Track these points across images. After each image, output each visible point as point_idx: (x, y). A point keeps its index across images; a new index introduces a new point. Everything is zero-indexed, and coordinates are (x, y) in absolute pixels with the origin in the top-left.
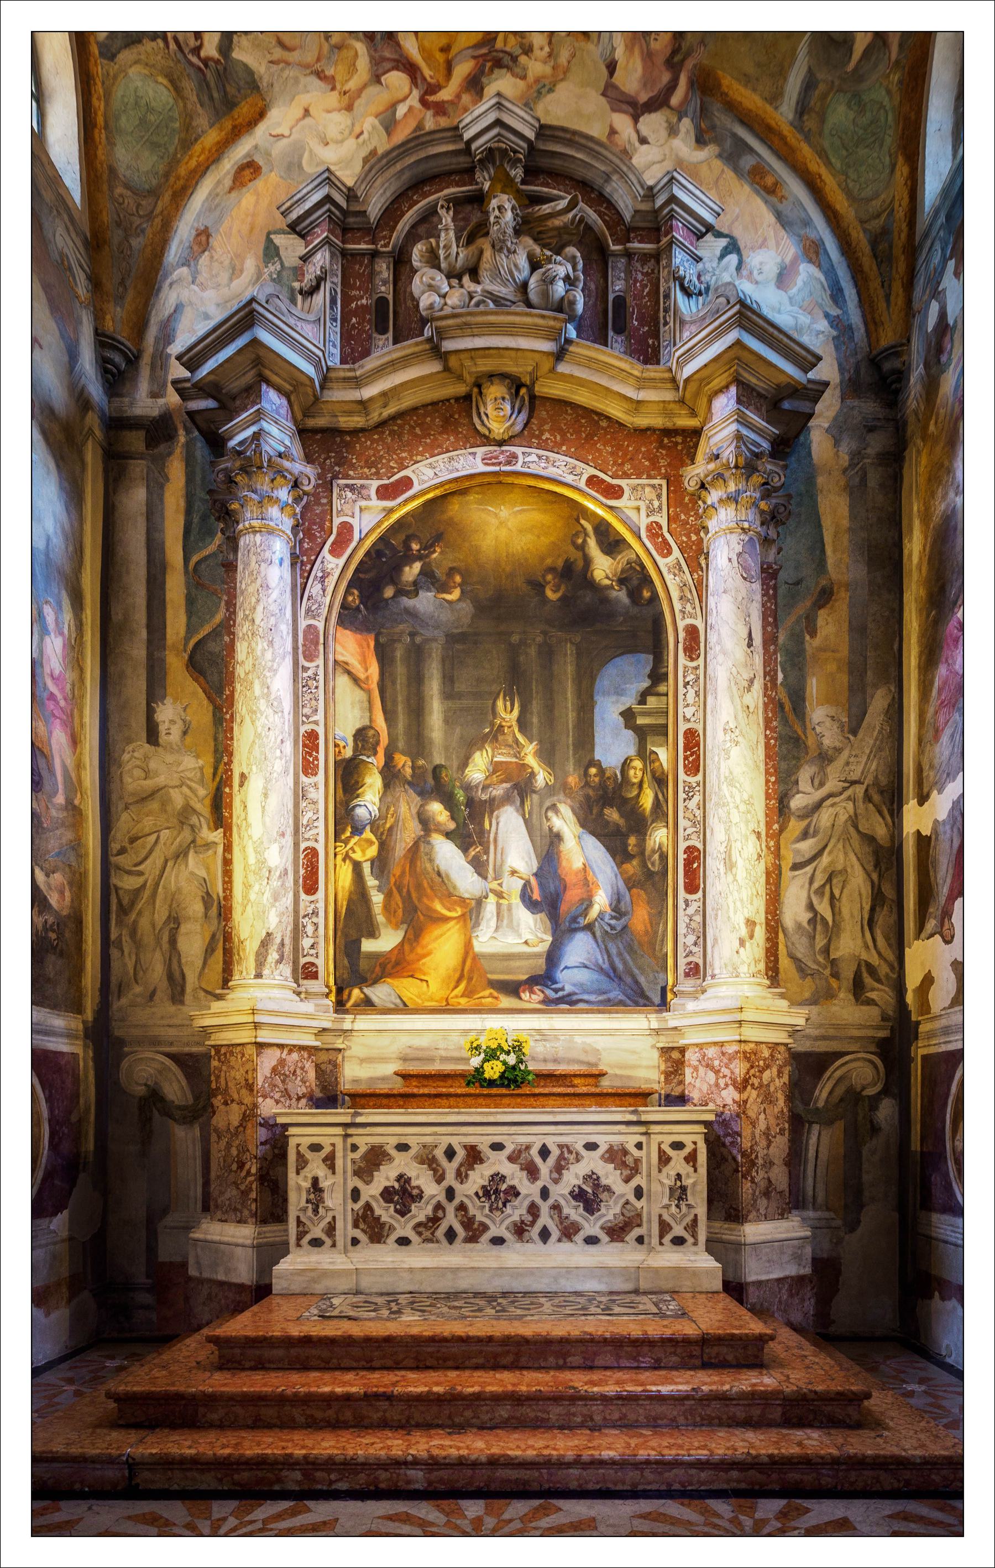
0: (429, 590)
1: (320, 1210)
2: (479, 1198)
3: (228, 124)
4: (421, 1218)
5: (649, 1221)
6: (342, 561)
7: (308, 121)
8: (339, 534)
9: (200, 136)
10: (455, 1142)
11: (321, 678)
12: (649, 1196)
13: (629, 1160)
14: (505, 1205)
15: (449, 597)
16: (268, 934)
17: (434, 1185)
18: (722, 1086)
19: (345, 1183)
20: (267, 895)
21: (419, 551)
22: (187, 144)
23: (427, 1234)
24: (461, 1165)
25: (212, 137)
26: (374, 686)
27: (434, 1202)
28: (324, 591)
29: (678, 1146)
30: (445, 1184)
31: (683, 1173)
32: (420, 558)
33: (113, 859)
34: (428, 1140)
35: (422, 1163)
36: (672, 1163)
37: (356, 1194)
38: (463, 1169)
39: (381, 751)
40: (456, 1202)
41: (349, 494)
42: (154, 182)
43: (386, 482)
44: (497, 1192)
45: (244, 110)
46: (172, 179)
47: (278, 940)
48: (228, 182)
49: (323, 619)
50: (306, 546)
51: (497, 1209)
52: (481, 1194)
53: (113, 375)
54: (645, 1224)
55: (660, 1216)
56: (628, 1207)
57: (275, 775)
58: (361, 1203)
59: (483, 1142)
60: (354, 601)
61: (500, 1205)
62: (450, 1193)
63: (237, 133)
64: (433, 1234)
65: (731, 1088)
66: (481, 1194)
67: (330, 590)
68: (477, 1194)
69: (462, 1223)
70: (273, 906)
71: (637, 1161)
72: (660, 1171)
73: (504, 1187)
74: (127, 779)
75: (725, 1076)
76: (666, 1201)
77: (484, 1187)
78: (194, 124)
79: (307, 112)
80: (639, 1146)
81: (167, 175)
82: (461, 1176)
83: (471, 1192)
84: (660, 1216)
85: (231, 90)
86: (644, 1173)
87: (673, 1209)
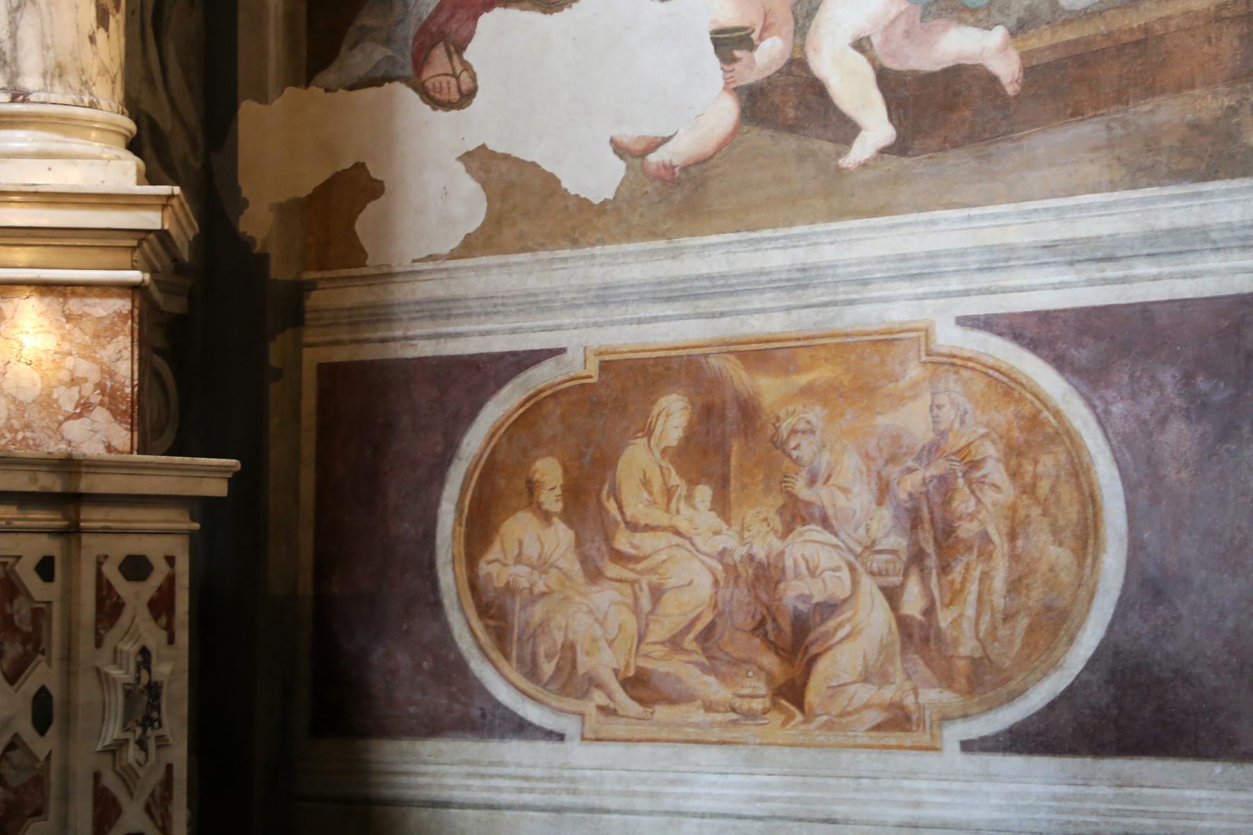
5: (66, 796)
12: (67, 719)
13: (20, 611)
18: (69, 407)
29: (136, 568)
31: (152, 645)
36: (124, 619)
54: (53, 808)
55: (97, 776)
56: (16, 756)
65: (101, 416)
71: (40, 614)
72: (99, 643)
75: (74, 382)
76: (113, 731)
80: (45, 568)
84: (97, 776)
86: (56, 650)
87: (132, 754)
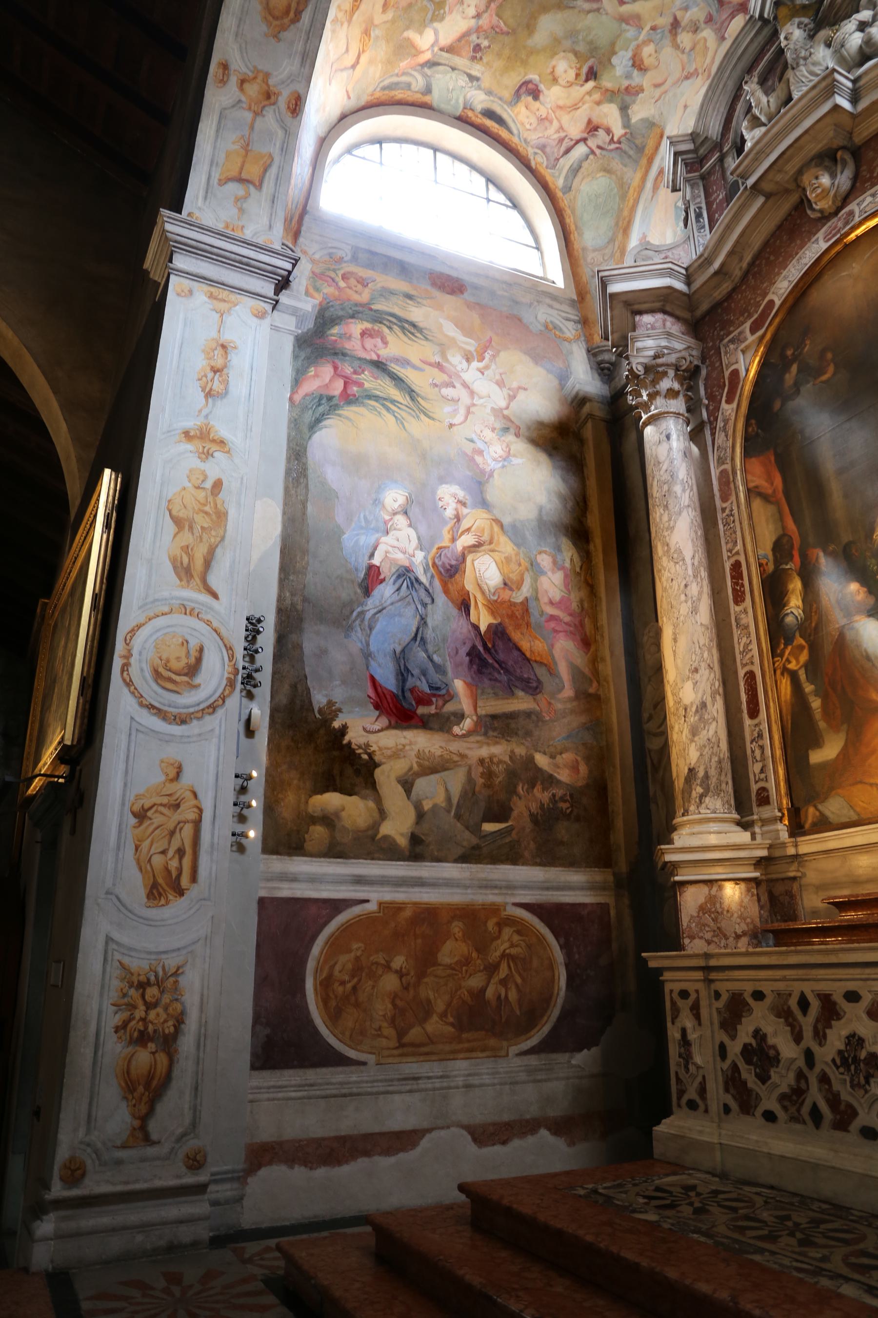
0: (808, 382)
1: (691, 1067)
2: (838, 1068)
3: (644, 161)
4: (784, 1088)
6: (735, 405)
7: (688, 110)
8: (730, 383)
9: (630, 184)
10: (808, 989)
11: (735, 511)
14: (868, 1082)
15: (825, 377)
16: (691, 770)
17: (793, 1044)
19: (713, 1037)
20: (686, 732)
21: (793, 354)
22: (623, 197)
23: (793, 1110)
24: (818, 1020)
25: (639, 175)
26: (781, 495)
27: (794, 1067)
28: (726, 436)
30: (804, 1044)
32: (795, 358)
33: (646, 727)
34: (781, 986)
35: (778, 1016)
37: (723, 1051)
38: (820, 1026)
39: (796, 553)
40: (817, 1069)
41: (732, 346)
42: (610, 234)
43: (756, 316)
44: (856, 1060)
45: (651, 144)
46: (621, 223)
47: (701, 774)
48: (651, 194)
49: (729, 461)
50: (711, 408)
51: (859, 1085)
52: (838, 1062)
53: (609, 369)
57: (682, 618)
58: (728, 1062)
59: (837, 991)
60: (753, 430)
61: (862, 1081)
62: (809, 1056)
63: (650, 161)
64: (798, 1111)
66: (838, 1062)
67: (730, 432)
68: (833, 1060)
69: (828, 1101)
70: (692, 741)
73: (863, 1055)
74: (648, 657)
77: (840, 1052)
78: (625, 180)
79: (686, 107)
81: (617, 224)
82: (820, 1037)
83: (829, 1059)
85: (638, 142)
